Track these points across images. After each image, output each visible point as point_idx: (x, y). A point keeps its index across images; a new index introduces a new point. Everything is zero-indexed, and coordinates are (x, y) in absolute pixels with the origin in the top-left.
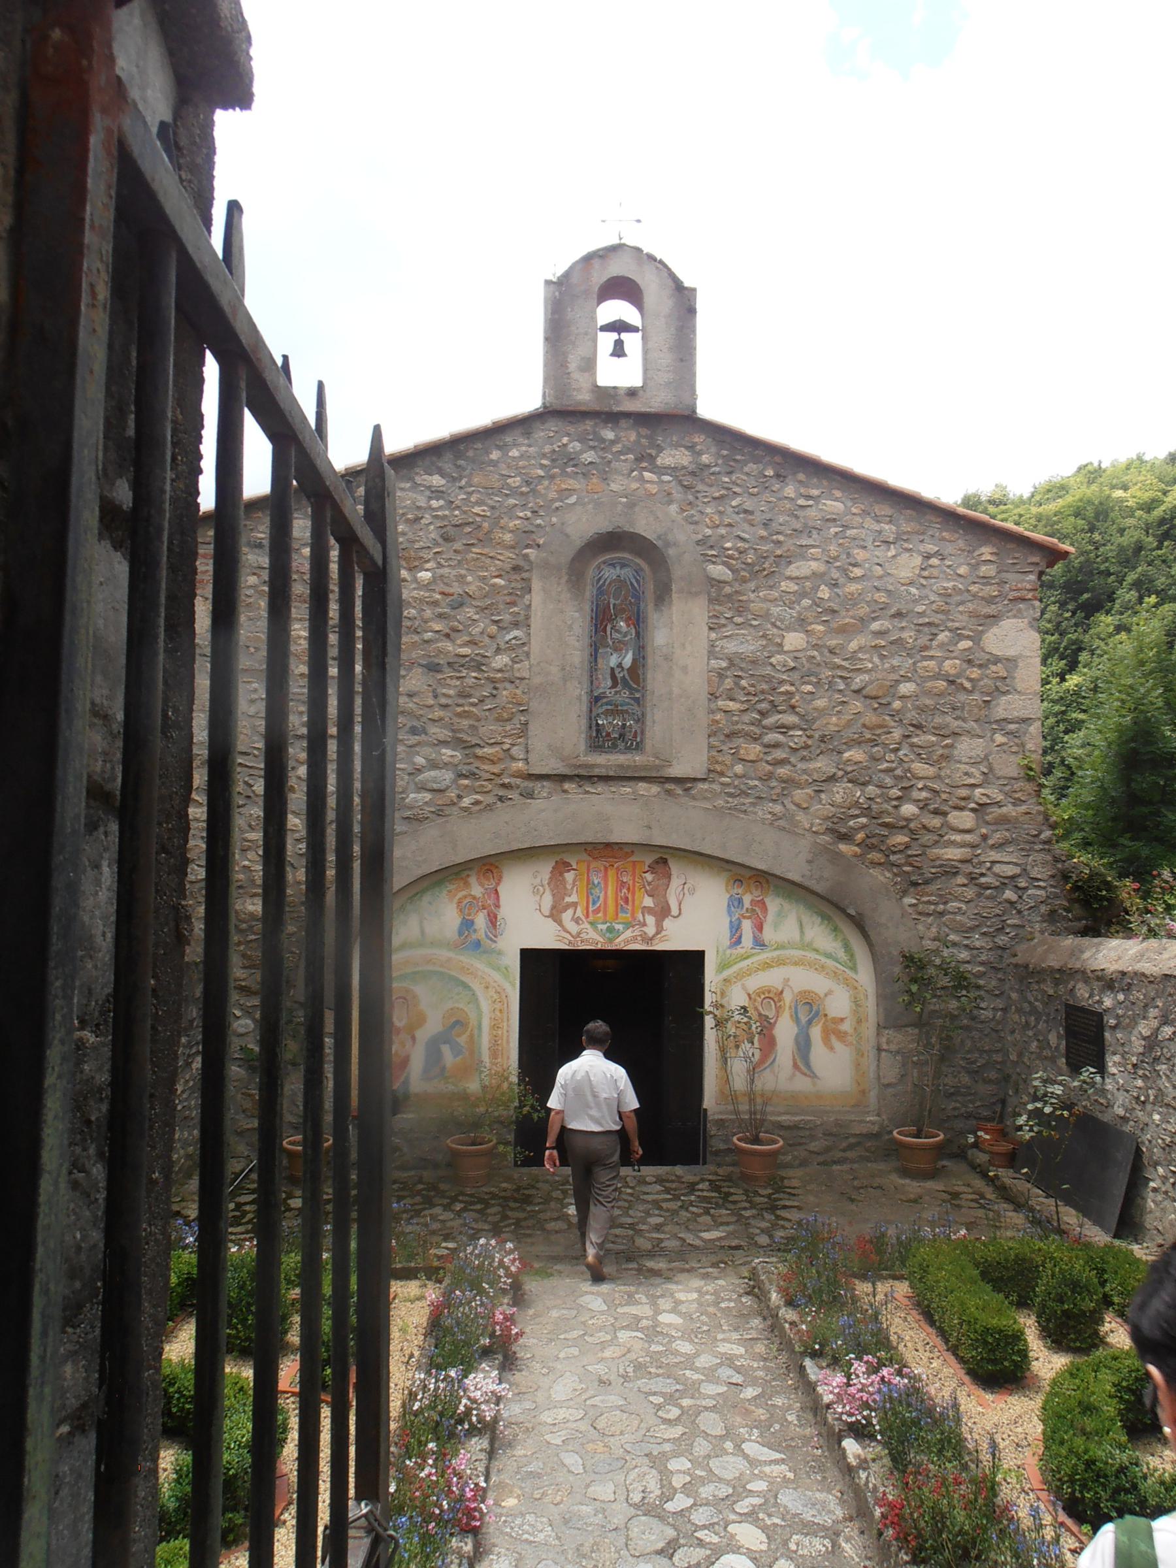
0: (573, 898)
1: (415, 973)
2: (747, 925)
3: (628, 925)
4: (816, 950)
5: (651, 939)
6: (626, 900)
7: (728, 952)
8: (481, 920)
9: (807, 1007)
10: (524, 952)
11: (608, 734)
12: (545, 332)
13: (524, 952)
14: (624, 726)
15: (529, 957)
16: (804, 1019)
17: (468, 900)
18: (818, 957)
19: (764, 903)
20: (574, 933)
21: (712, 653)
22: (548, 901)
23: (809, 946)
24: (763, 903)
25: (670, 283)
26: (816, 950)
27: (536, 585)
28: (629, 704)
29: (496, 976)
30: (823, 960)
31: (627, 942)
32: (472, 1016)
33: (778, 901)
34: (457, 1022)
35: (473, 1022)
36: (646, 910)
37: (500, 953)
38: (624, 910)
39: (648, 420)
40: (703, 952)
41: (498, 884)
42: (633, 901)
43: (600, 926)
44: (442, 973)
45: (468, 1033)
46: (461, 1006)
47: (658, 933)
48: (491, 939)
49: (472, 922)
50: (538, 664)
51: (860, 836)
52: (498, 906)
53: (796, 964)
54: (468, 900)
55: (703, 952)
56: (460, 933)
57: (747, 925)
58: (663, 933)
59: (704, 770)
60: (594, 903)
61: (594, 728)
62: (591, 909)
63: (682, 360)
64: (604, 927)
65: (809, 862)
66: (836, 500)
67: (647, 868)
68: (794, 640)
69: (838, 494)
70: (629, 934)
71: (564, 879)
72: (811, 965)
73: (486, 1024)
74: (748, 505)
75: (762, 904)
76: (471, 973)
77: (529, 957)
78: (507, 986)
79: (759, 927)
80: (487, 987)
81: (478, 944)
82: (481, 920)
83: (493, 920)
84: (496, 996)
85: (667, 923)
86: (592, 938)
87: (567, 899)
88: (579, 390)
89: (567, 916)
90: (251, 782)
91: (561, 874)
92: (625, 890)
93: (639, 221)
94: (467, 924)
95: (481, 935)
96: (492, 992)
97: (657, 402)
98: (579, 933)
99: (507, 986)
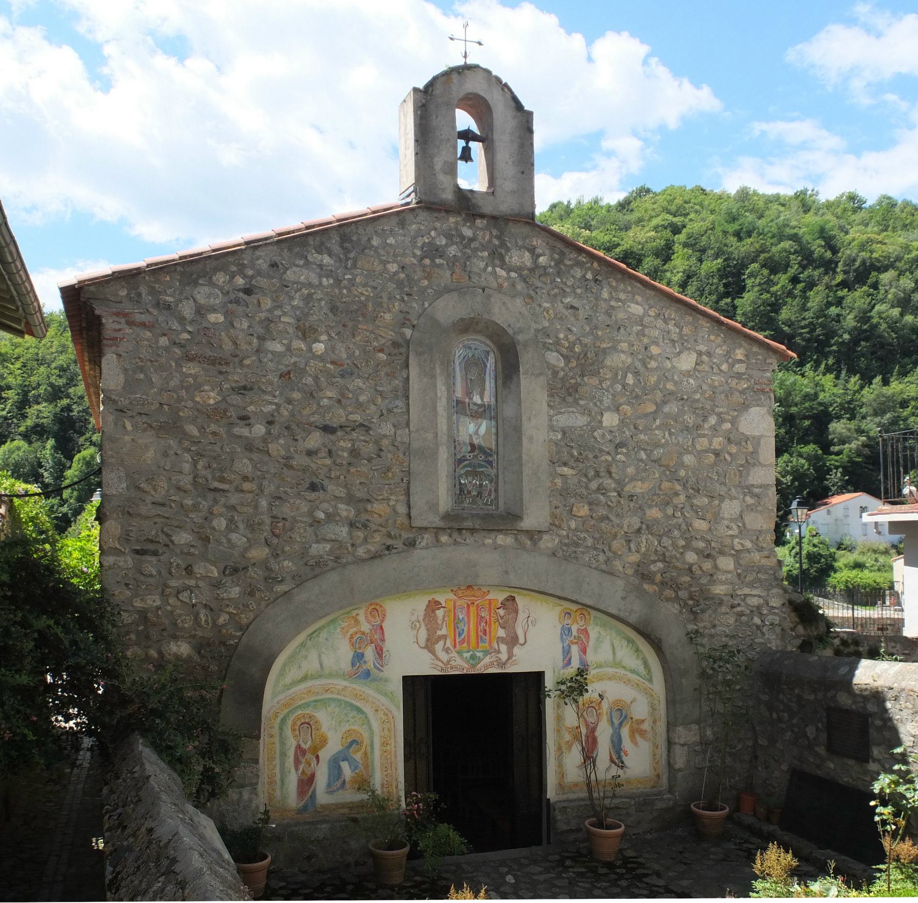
0: (443, 632)
1: (316, 701)
2: (575, 649)
3: (486, 653)
4: (624, 667)
5: (505, 664)
6: (485, 632)
7: (562, 671)
8: (369, 653)
9: (619, 712)
10: (406, 679)
11: (469, 492)
12: (416, 135)
13: (406, 679)
14: (481, 485)
15: (409, 682)
16: (616, 722)
17: (358, 635)
18: (626, 673)
19: (587, 632)
20: (445, 660)
21: (552, 428)
22: (423, 634)
23: (617, 664)
24: (586, 631)
25: (513, 104)
26: (624, 667)
27: (412, 361)
28: (483, 466)
29: (383, 699)
30: (630, 675)
31: (487, 667)
32: (366, 735)
33: (597, 629)
34: (354, 741)
35: (366, 741)
36: (500, 640)
37: (386, 680)
38: (483, 641)
39: (497, 220)
40: (543, 672)
41: (382, 621)
42: (490, 632)
43: (465, 655)
44: (339, 700)
45: (363, 750)
46: (355, 727)
47: (509, 658)
48: (379, 670)
49: (363, 655)
50: (417, 430)
51: (658, 578)
52: (383, 640)
53: (610, 679)
54: (358, 635)
55: (543, 672)
56: (353, 665)
57: (575, 649)
58: (514, 658)
59: (547, 524)
60: (460, 635)
61: (457, 486)
62: (457, 641)
63: (523, 173)
64: (468, 655)
65: (623, 598)
66: (637, 303)
67: (500, 605)
68: (610, 420)
69: (639, 298)
70: (487, 660)
71: (435, 615)
72: (620, 679)
73: (377, 741)
74: (576, 303)
75: (585, 632)
76: (364, 699)
77: (409, 682)
78: (393, 708)
79: (584, 651)
80: (377, 710)
81: (368, 674)
82: (369, 653)
83: (379, 652)
84: (384, 718)
85: (516, 650)
86: (459, 665)
87: (439, 633)
88: (443, 190)
89: (439, 647)
90: (169, 532)
91: (433, 611)
92: (483, 624)
93: (480, 44)
94: (359, 657)
95: (370, 665)
96: (381, 715)
97: (506, 205)
98: (449, 661)
99: (393, 708)
